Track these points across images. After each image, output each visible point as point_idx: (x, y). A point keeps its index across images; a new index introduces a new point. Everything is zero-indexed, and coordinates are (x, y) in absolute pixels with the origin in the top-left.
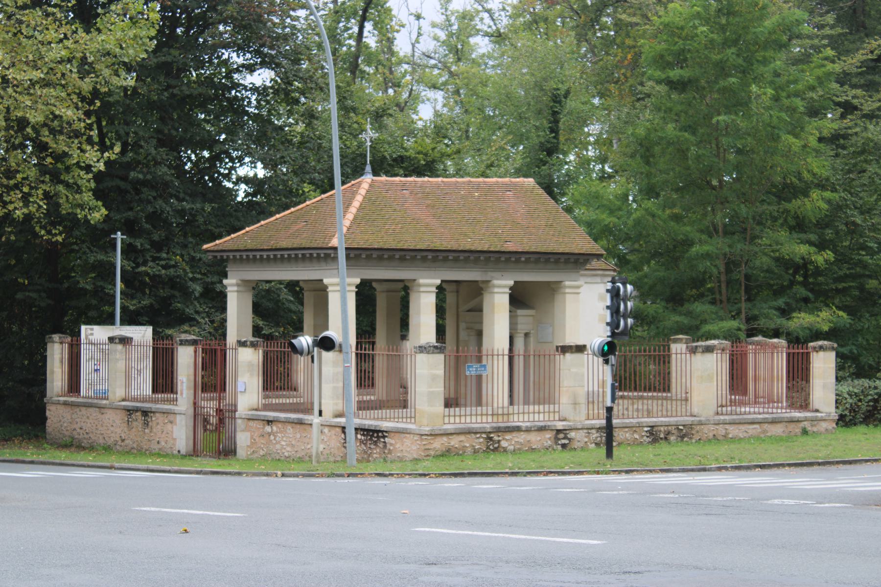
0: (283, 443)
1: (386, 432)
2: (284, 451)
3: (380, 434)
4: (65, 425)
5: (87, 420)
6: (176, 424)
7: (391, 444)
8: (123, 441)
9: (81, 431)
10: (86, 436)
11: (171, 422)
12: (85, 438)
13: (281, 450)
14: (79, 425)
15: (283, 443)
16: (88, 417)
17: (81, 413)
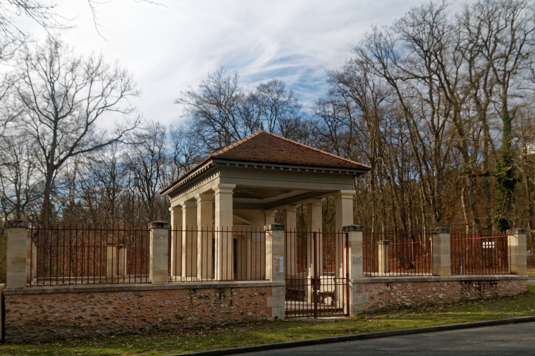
0: (403, 297)
1: (497, 280)
2: (404, 302)
3: (493, 282)
4: (57, 315)
5: (108, 306)
6: (271, 295)
7: (501, 287)
8: (181, 318)
9: (93, 319)
10: (104, 322)
11: (262, 295)
12: (102, 325)
13: (401, 302)
14: (88, 312)
15: (403, 297)
16: (110, 303)
17: (92, 300)
